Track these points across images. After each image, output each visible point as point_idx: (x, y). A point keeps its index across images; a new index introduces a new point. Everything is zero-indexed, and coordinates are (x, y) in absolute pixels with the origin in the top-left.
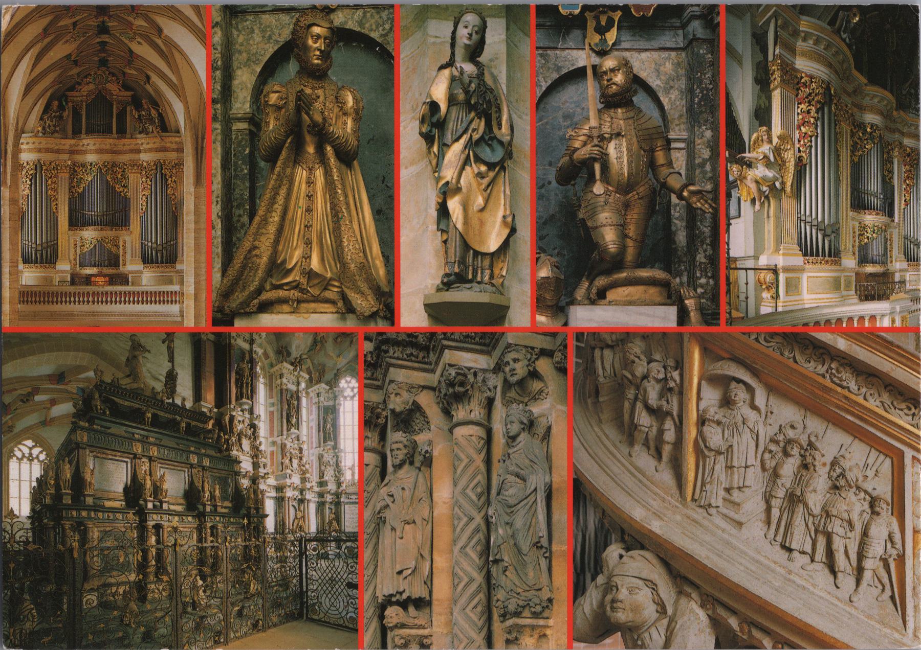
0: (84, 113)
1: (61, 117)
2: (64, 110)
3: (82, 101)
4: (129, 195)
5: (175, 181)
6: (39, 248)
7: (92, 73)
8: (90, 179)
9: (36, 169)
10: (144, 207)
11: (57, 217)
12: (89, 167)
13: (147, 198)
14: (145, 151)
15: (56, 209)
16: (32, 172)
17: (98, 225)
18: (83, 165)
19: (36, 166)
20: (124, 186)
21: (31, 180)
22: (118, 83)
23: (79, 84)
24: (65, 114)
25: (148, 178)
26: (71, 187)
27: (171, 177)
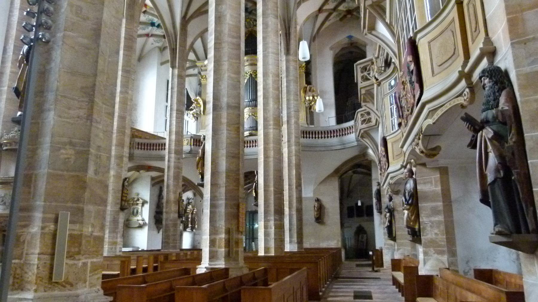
8: (246, 82)
17: (250, 106)
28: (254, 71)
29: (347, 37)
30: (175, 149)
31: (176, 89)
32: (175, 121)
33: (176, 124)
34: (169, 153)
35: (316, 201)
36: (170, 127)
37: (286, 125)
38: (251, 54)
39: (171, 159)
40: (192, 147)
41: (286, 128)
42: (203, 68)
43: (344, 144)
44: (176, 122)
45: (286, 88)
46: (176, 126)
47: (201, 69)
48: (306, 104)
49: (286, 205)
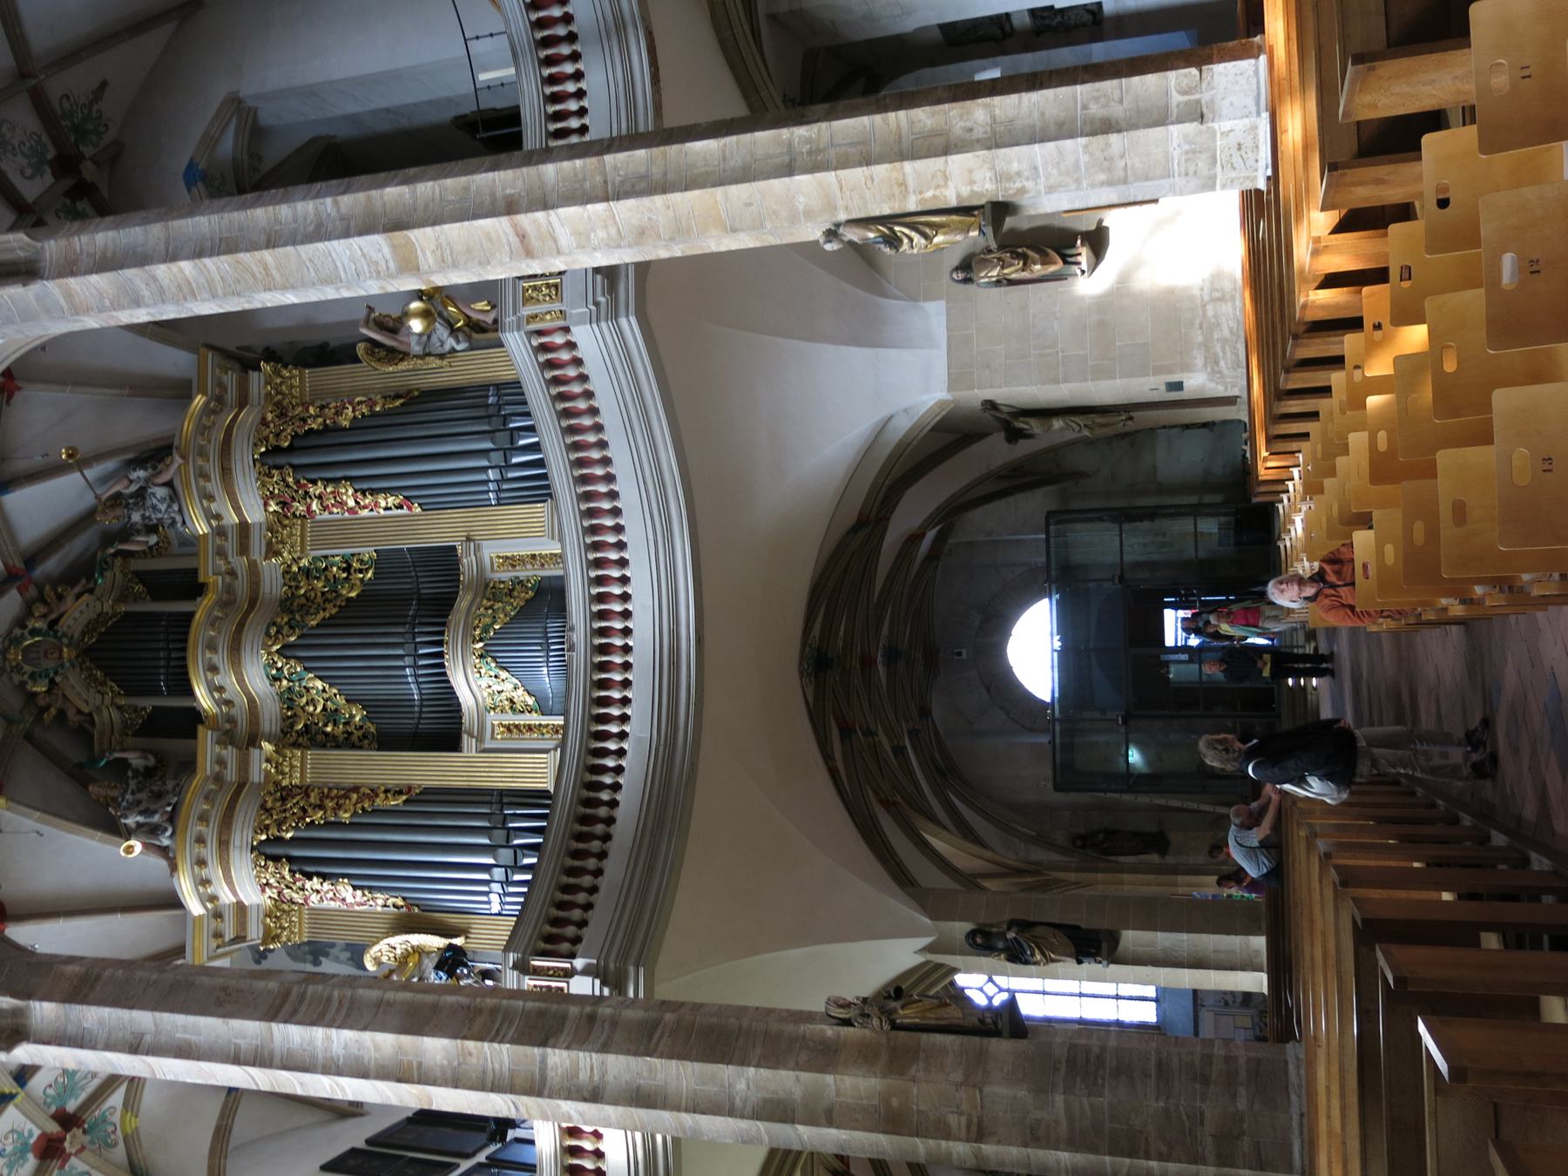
0: (148, 703)
1: (149, 773)
2: (124, 763)
3: (120, 708)
4: (368, 552)
5: (322, 407)
6: (506, 855)
7: (17, 678)
8: (319, 684)
9: (276, 859)
10: (391, 500)
11: (428, 791)
12: (285, 682)
13: (364, 492)
14: (237, 510)
15: (400, 793)
16: (286, 873)
18: (288, 698)
19: (269, 857)
20: (348, 569)
21: (309, 876)
22: (60, 598)
23: (62, 714)
24: (135, 759)
25: (307, 493)
26: (349, 742)
27: (304, 420)
28: (268, 634)
29: (189, 191)
30: (514, 1041)
31: (143, 1019)
32: (333, 1032)
33: (351, 1028)
34: (536, 1087)
35: (967, 281)
36: (364, 1075)
37: (415, 235)
38: (184, 649)
39: (583, 1076)
40: (579, 963)
41: (428, 230)
42: (229, 934)
43: (620, 27)
44: (341, 1027)
45: (208, 262)
46: (365, 1028)
47: (234, 941)
48: (453, 350)
49: (929, 194)
